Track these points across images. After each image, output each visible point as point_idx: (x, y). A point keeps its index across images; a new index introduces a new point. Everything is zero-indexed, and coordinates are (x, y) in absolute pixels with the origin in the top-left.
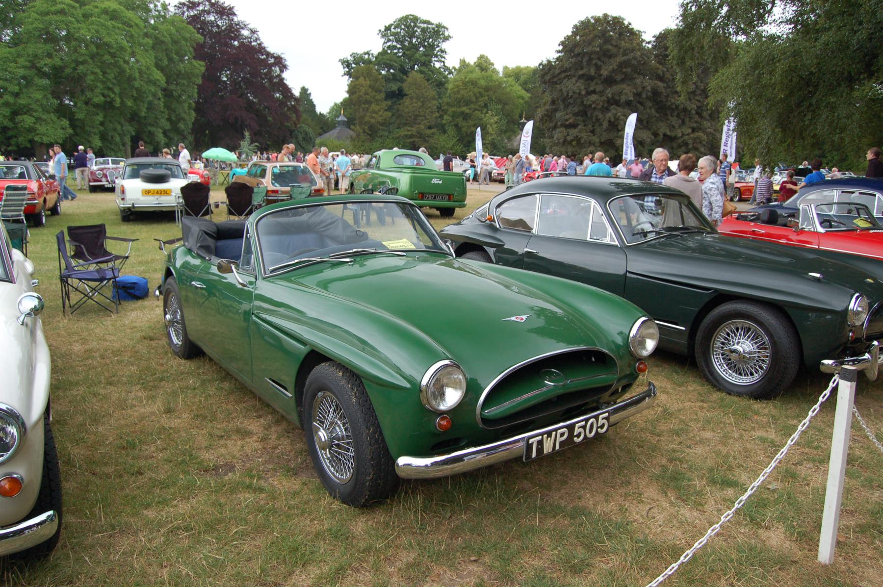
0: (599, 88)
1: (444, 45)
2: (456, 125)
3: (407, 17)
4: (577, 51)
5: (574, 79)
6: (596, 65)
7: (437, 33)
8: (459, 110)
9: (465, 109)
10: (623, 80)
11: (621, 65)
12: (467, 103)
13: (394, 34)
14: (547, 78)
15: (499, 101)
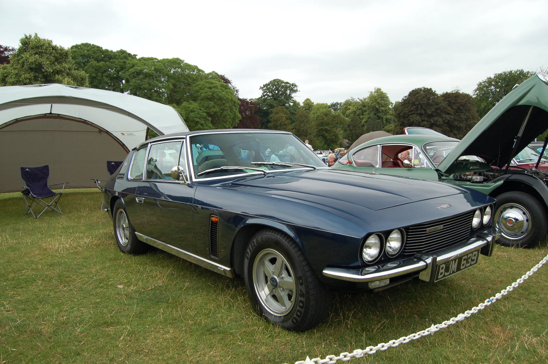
0: (426, 119)
1: (293, 95)
2: (323, 136)
3: (274, 80)
4: (417, 103)
5: (415, 115)
6: (424, 109)
7: (292, 88)
8: (323, 128)
9: (326, 127)
10: (436, 116)
11: (437, 109)
12: (328, 124)
13: (268, 89)
14: (402, 114)
15: (341, 123)
